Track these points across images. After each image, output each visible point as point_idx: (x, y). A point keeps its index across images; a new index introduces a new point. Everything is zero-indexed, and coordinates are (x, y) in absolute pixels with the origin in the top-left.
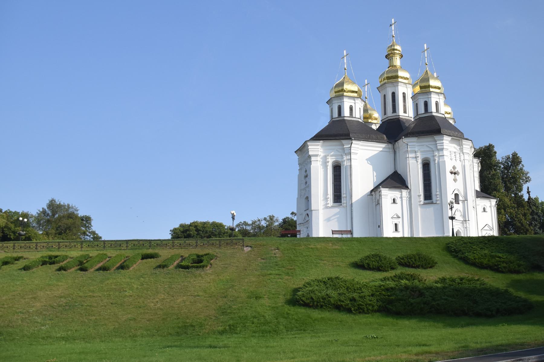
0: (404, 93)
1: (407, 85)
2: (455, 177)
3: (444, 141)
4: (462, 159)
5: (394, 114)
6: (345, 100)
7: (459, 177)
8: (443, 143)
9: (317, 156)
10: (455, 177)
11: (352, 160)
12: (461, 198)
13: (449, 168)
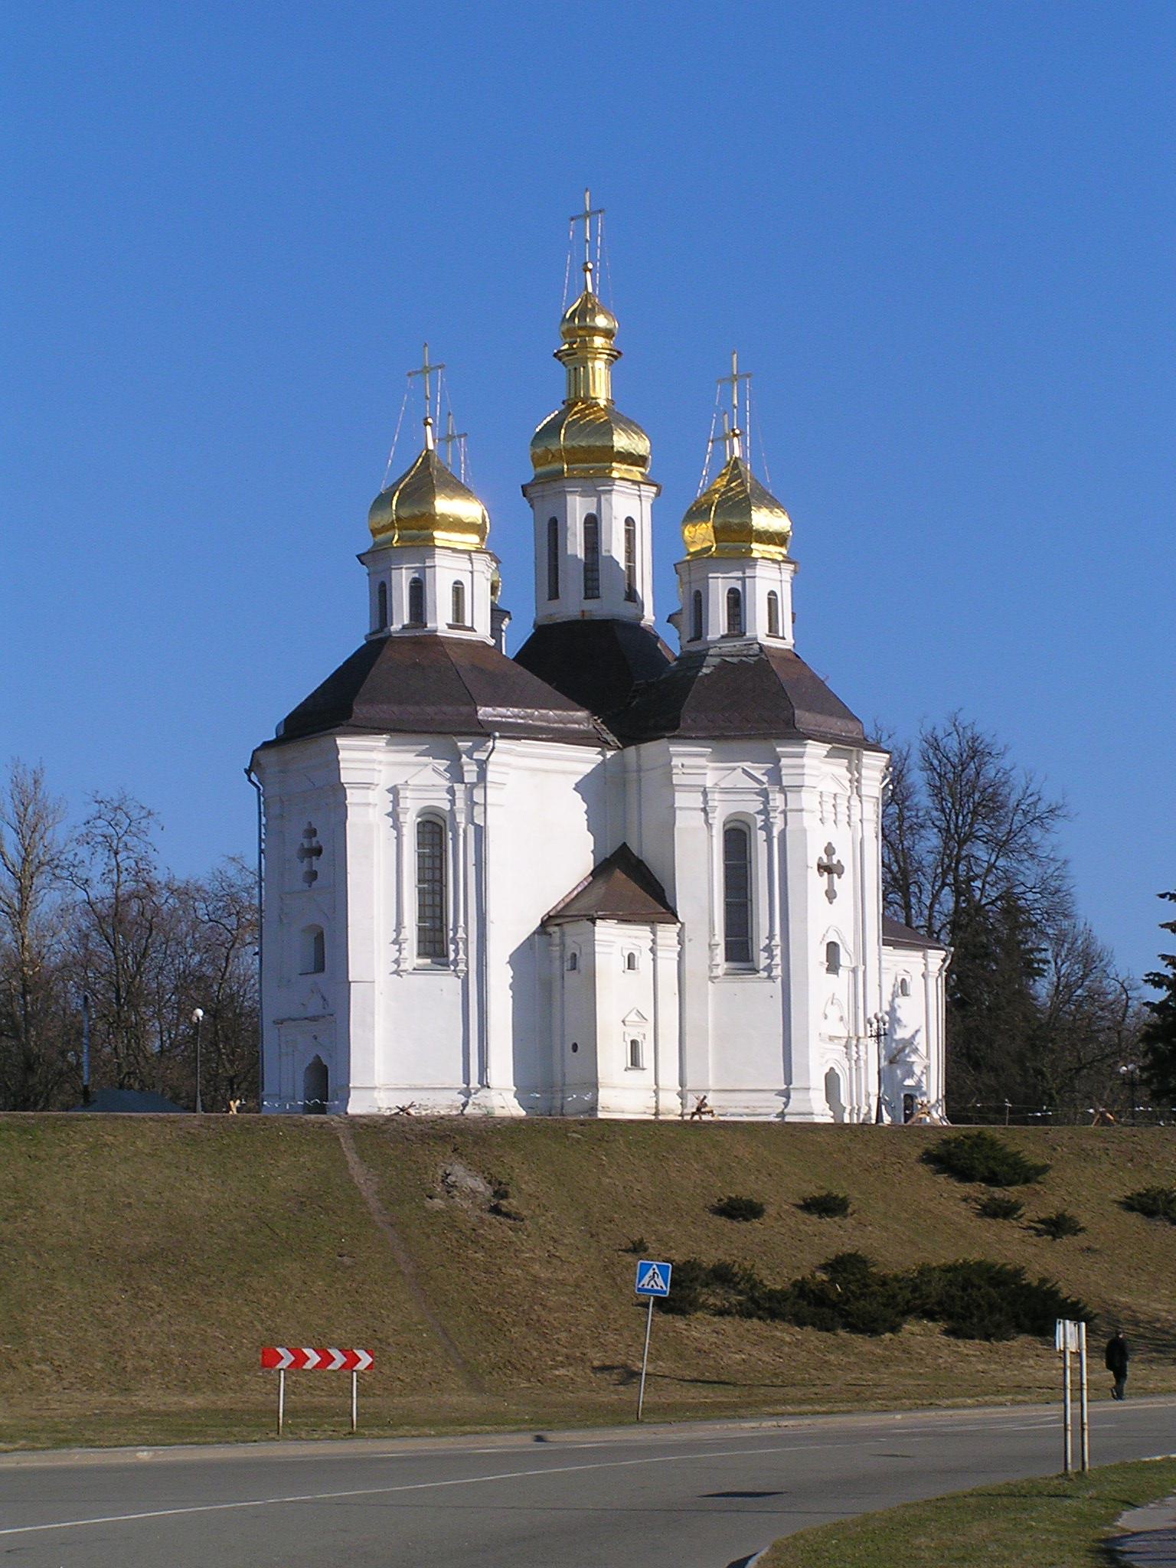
0: (629, 521)
1: (642, 486)
2: (831, 883)
3: (806, 761)
4: (855, 818)
5: (591, 606)
6: (441, 559)
7: (844, 885)
8: (803, 766)
9: (367, 786)
10: (831, 883)
11: (488, 807)
12: (844, 959)
13: (815, 853)
